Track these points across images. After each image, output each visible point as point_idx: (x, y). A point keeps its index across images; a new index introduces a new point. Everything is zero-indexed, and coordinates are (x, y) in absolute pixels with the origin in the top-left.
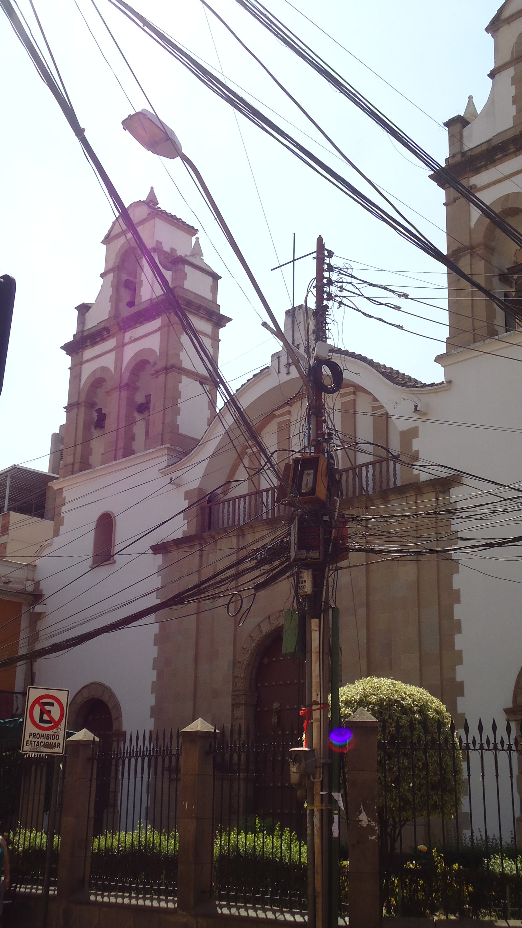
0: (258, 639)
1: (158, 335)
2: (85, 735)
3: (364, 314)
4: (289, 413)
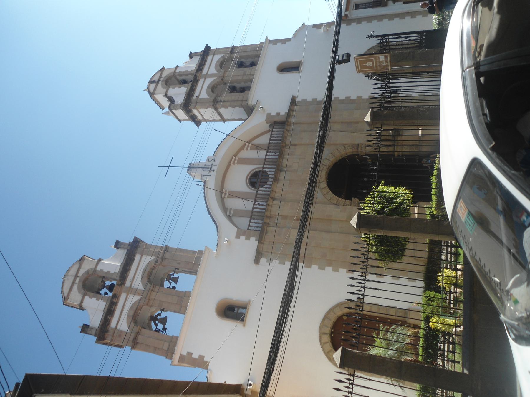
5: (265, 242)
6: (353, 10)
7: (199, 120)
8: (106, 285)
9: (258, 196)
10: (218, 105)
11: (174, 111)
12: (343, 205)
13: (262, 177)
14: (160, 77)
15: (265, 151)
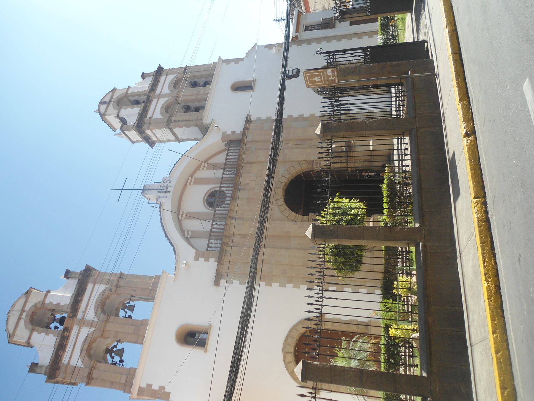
1: (97, 286)
4: (183, 212)
5: (225, 263)
6: (303, 31)
7: (153, 141)
8: (56, 318)
9: (216, 216)
10: (172, 125)
11: (126, 132)
12: (301, 220)
13: (220, 197)
14: (112, 98)
15: (222, 171)
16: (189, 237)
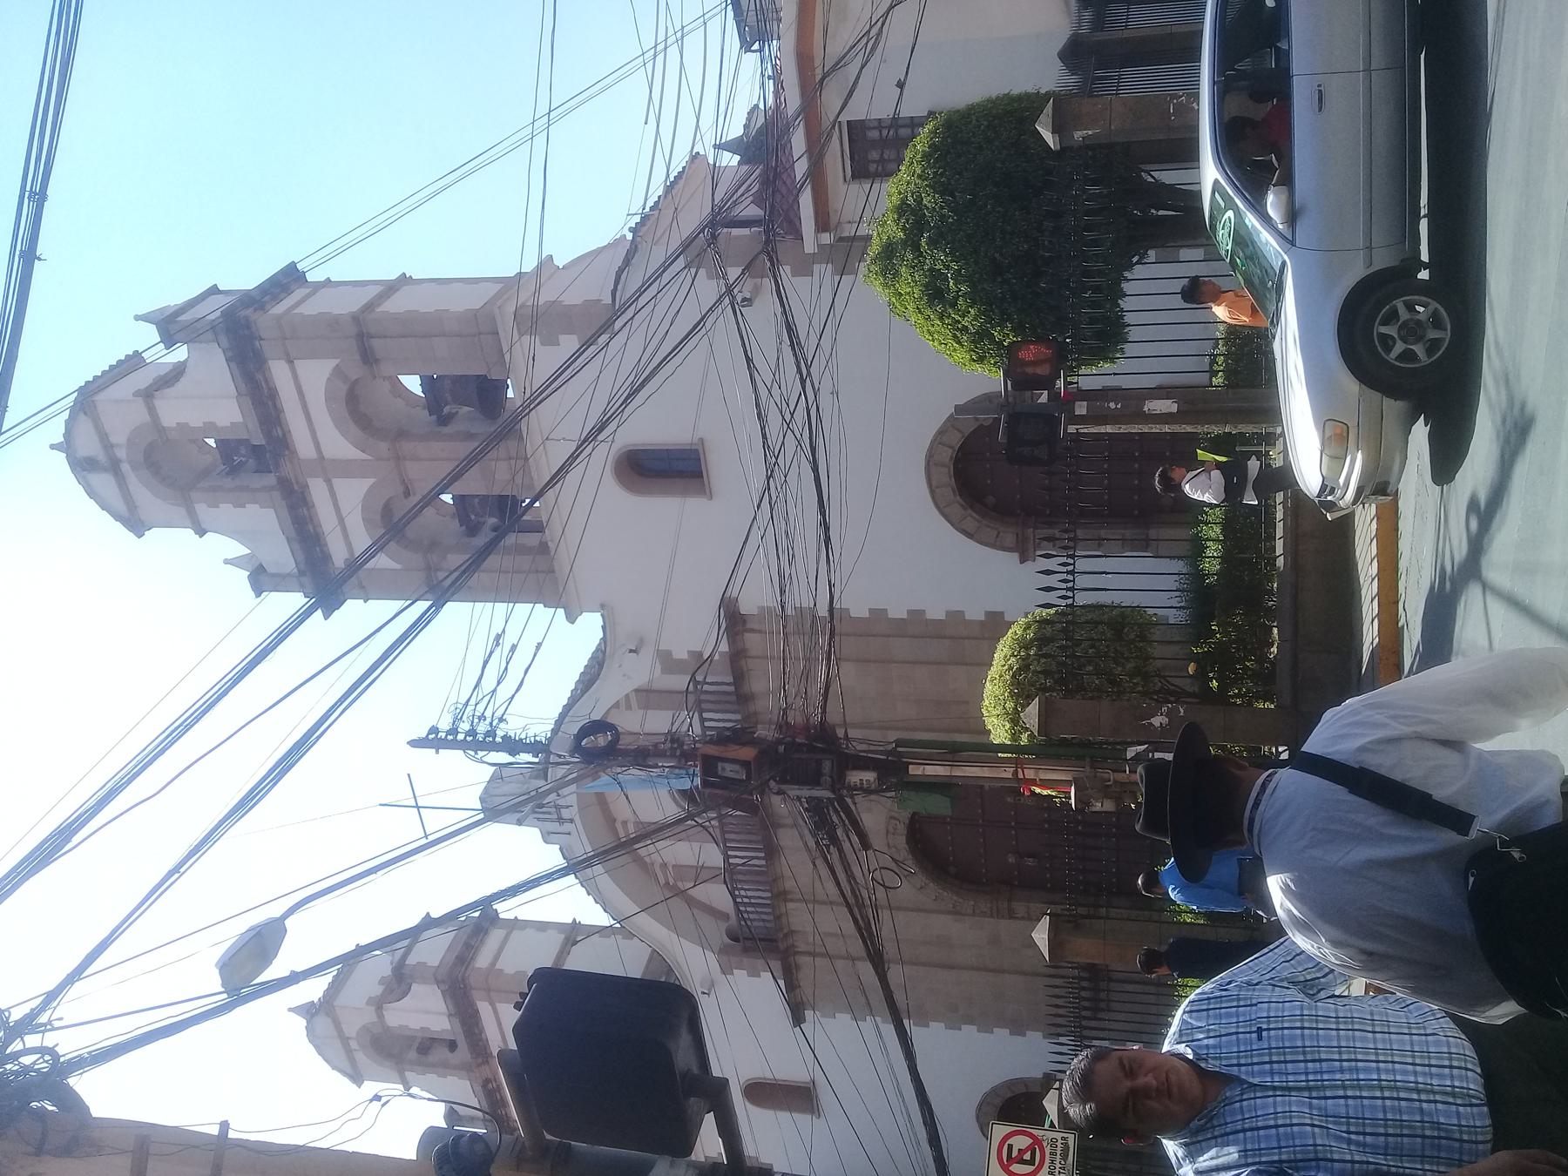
0: (924, 879)
2: (1051, 1102)
3: (517, 690)
12: (970, 911)
14: (108, 446)
16: (671, 882)
